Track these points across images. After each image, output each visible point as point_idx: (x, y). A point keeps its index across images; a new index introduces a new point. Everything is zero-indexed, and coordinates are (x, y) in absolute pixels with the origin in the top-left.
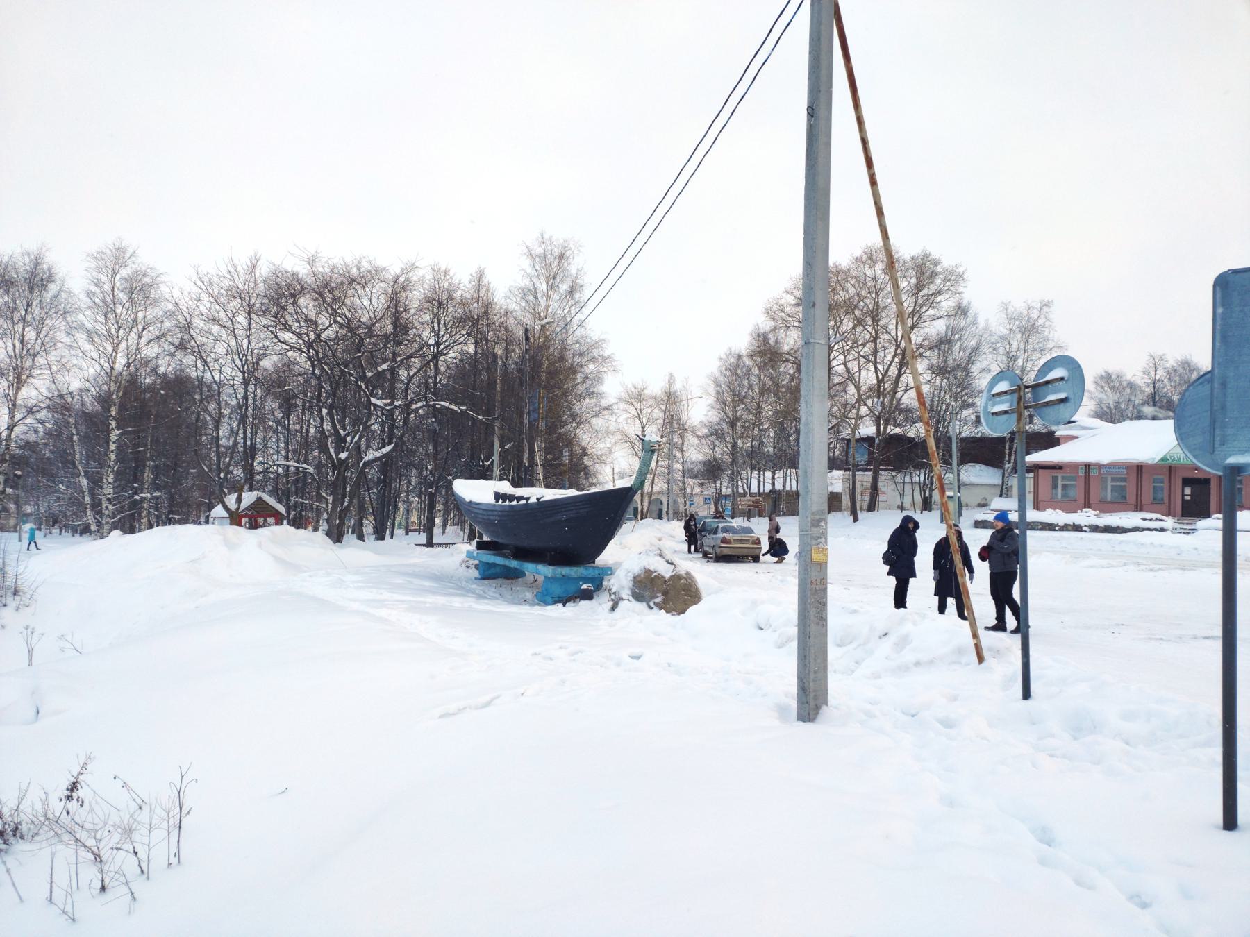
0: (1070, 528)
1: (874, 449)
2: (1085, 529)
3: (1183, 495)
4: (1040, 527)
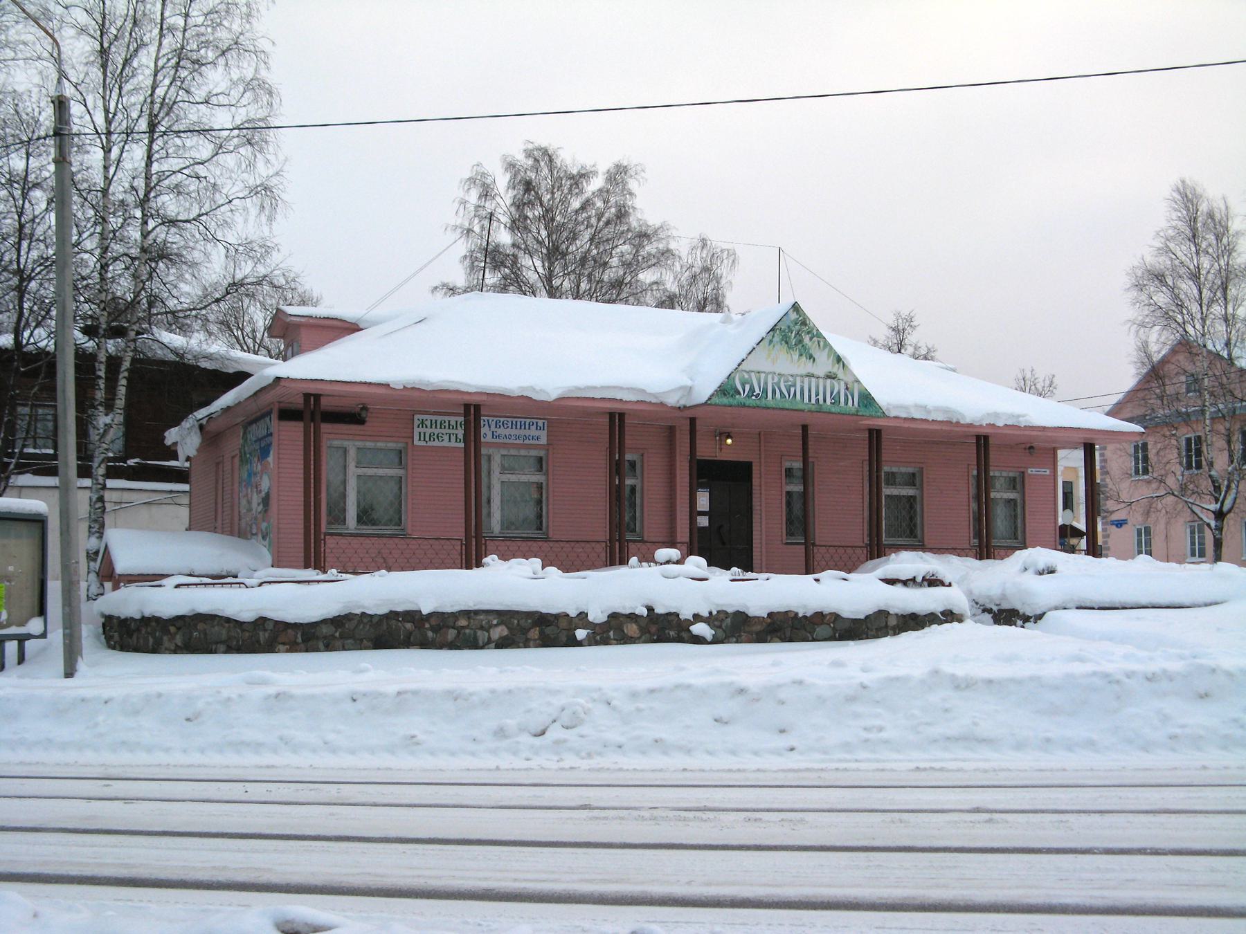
0: (632, 629)
1: (11, 463)
2: (700, 629)
3: (694, 513)
4: (499, 632)
